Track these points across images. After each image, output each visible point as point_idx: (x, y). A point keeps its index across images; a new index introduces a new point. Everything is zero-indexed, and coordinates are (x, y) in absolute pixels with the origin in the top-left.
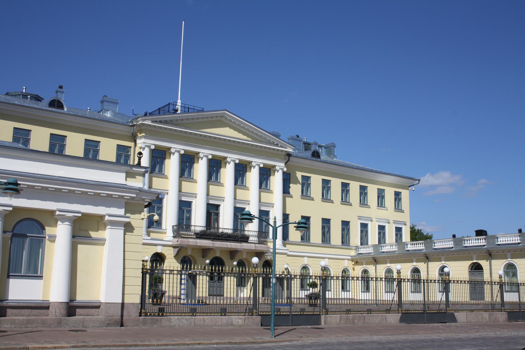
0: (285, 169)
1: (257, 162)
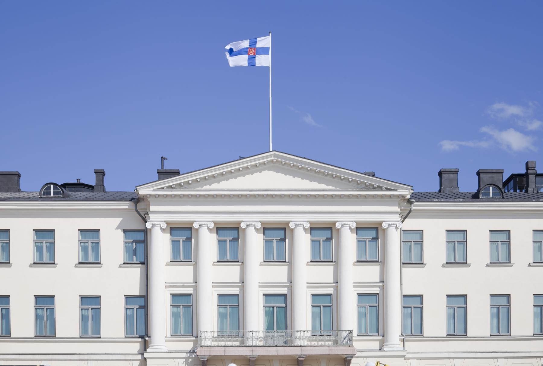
1: (346, 218)
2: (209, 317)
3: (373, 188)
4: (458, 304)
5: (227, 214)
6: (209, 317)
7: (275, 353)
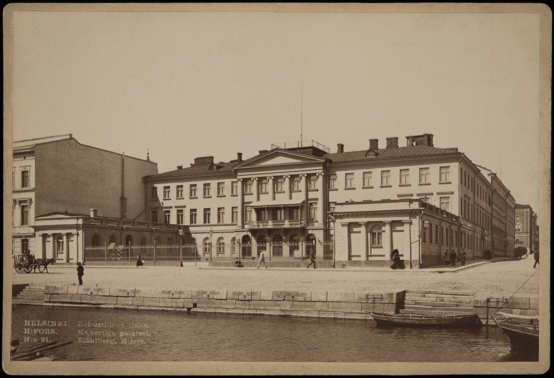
0: (323, 174)
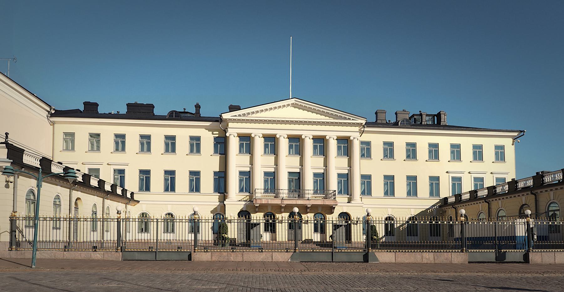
2: (259, 183)
3: (345, 119)
4: (389, 180)
5: (270, 129)
6: (259, 183)
7: (295, 203)
